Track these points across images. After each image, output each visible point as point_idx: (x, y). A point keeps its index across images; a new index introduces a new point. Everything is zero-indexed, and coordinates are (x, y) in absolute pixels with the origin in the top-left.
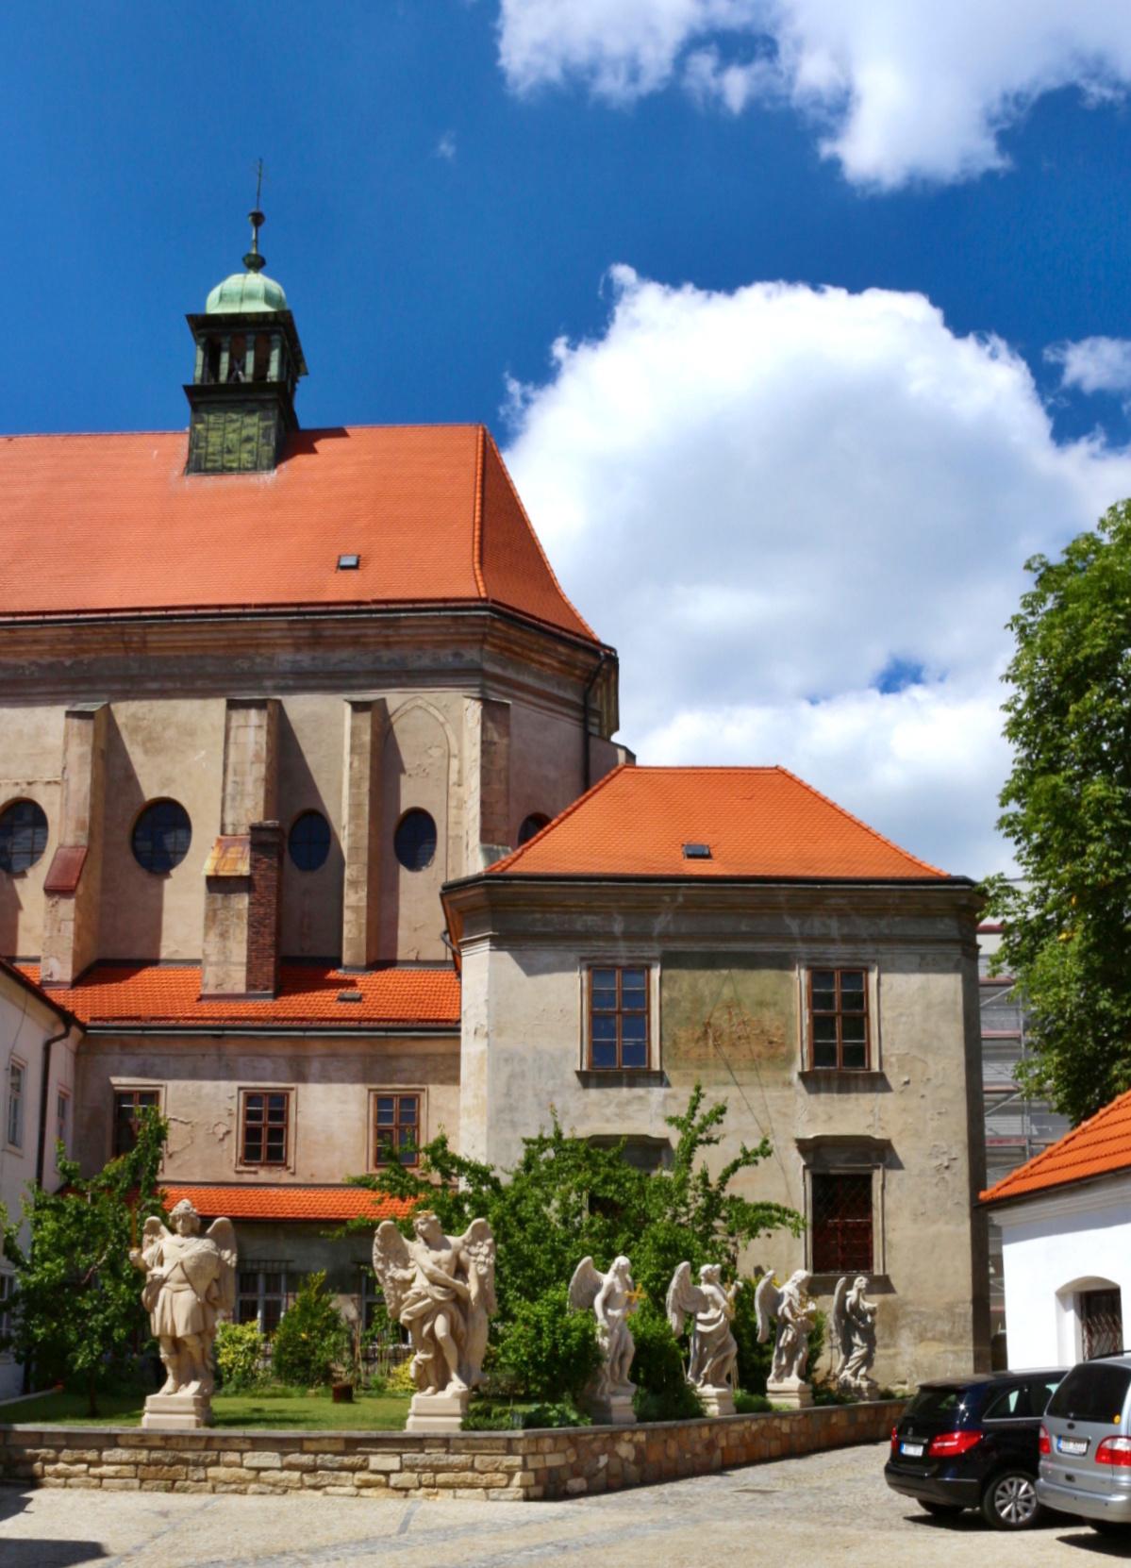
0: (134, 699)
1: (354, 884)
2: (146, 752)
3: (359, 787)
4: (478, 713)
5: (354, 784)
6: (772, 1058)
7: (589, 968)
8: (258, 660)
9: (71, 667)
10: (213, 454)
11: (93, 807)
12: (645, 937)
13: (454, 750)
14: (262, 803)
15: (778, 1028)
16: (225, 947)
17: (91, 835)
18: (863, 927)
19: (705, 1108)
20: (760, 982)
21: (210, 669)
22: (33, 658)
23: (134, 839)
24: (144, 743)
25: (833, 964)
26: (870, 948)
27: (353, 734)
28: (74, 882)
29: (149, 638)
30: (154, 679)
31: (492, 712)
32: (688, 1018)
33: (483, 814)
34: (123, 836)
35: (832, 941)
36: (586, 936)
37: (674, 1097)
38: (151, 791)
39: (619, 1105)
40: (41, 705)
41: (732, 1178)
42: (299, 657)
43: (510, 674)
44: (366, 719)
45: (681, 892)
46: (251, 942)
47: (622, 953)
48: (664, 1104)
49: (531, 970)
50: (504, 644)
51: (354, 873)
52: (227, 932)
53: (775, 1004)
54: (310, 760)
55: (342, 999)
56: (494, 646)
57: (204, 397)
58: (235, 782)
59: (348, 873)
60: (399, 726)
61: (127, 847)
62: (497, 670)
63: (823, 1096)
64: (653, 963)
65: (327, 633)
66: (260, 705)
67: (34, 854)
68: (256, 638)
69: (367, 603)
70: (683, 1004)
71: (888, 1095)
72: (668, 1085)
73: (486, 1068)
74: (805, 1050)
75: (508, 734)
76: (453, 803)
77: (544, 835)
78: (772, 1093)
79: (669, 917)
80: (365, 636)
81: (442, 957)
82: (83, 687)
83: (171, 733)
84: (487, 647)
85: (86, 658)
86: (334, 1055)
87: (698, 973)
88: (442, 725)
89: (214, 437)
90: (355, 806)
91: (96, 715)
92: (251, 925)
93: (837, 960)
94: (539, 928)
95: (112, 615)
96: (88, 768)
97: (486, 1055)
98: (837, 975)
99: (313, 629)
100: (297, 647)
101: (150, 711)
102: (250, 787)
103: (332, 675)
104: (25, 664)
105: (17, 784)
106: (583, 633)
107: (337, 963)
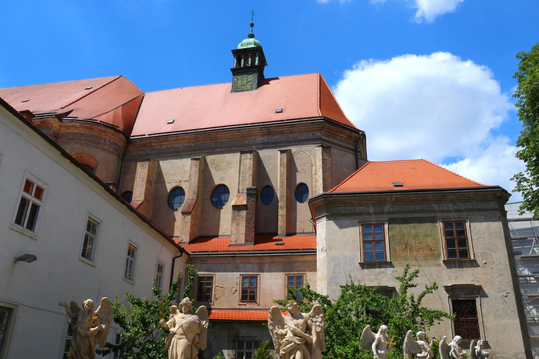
0: (212, 154)
1: (282, 208)
2: (216, 170)
3: (283, 177)
4: (321, 151)
5: (281, 176)
6: (432, 256)
7: (362, 225)
8: (251, 140)
9: (194, 146)
11: (198, 187)
12: (382, 213)
13: (314, 164)
15: (433, 244)
16: (238, 228)
17: (198, 196)
18: (462, 206)
19: (411, 270)
20: (425, 227)
21: (236, 144)
22: (183, 144)
23: (212, 197)
24: (215, 168)
25: (452, 220)
26: (465, 213)
27: (281, 160)
28: (191, 210)
29: (217, 136)
30: (219, 148)
31: (326, 149)
32: (399, 242)
33: (323, 182)
34: (208, 196)
35: (451, 211)
36: (360, 214)
37: (396, 271)
38: (217, 182)
39: (376, 275)
40: (185, 158)
41: (423, 299)
42: (263, 139)
43: (331, 140)
44: (285, 155)
45: (394, 196)
46: (246, 226)
47: (374, 219)
48: (392, 274)
49: (341, 227)
50: (328, 130)
51: (282, 204)
52: (239, 223)
53: (431, 236)
54: (267, 169)
55: (276, 245)
56: (325, 131)
57: (236, 72)
58: (243, 176)
59: (280, 204)
60: (295, 157)
61: (209, 200)
62: (327, 139)
63: (453, 269)
64: (385, 222)
65: (272, 131)
66: (251, 152)
67: (181, 203)
68: (251, 134)
69: (285, 121)
70: (397, 237)
71: (479, 268)
72: (394, 267)
73: (326, 263)
74: (444, 252)
75: (331, 157)
76: (314, 180)
77: (344, 183)
78: (433, 269)
79: (390, 205)
80: (284, 130)
81: (312, 231)
82: (197, 152)
83: (224, 164)
84: (323, 132)
85: (198, 143)
86: (273, 262)
87: (402, 225)
89: (239, 82)
90: (282, 183)
91: (200, 159)
92: (246, 221)
93: (453, 218)
94: (343, 212)
96: (197, 175)
97: (326, 258)
98: (454, 224)
99: (268, 130)
100: (263, 135)
101: (218, 158)
103: (273, 143)
104: (181, 146)
105: (176, 182)
107: (276, 234)
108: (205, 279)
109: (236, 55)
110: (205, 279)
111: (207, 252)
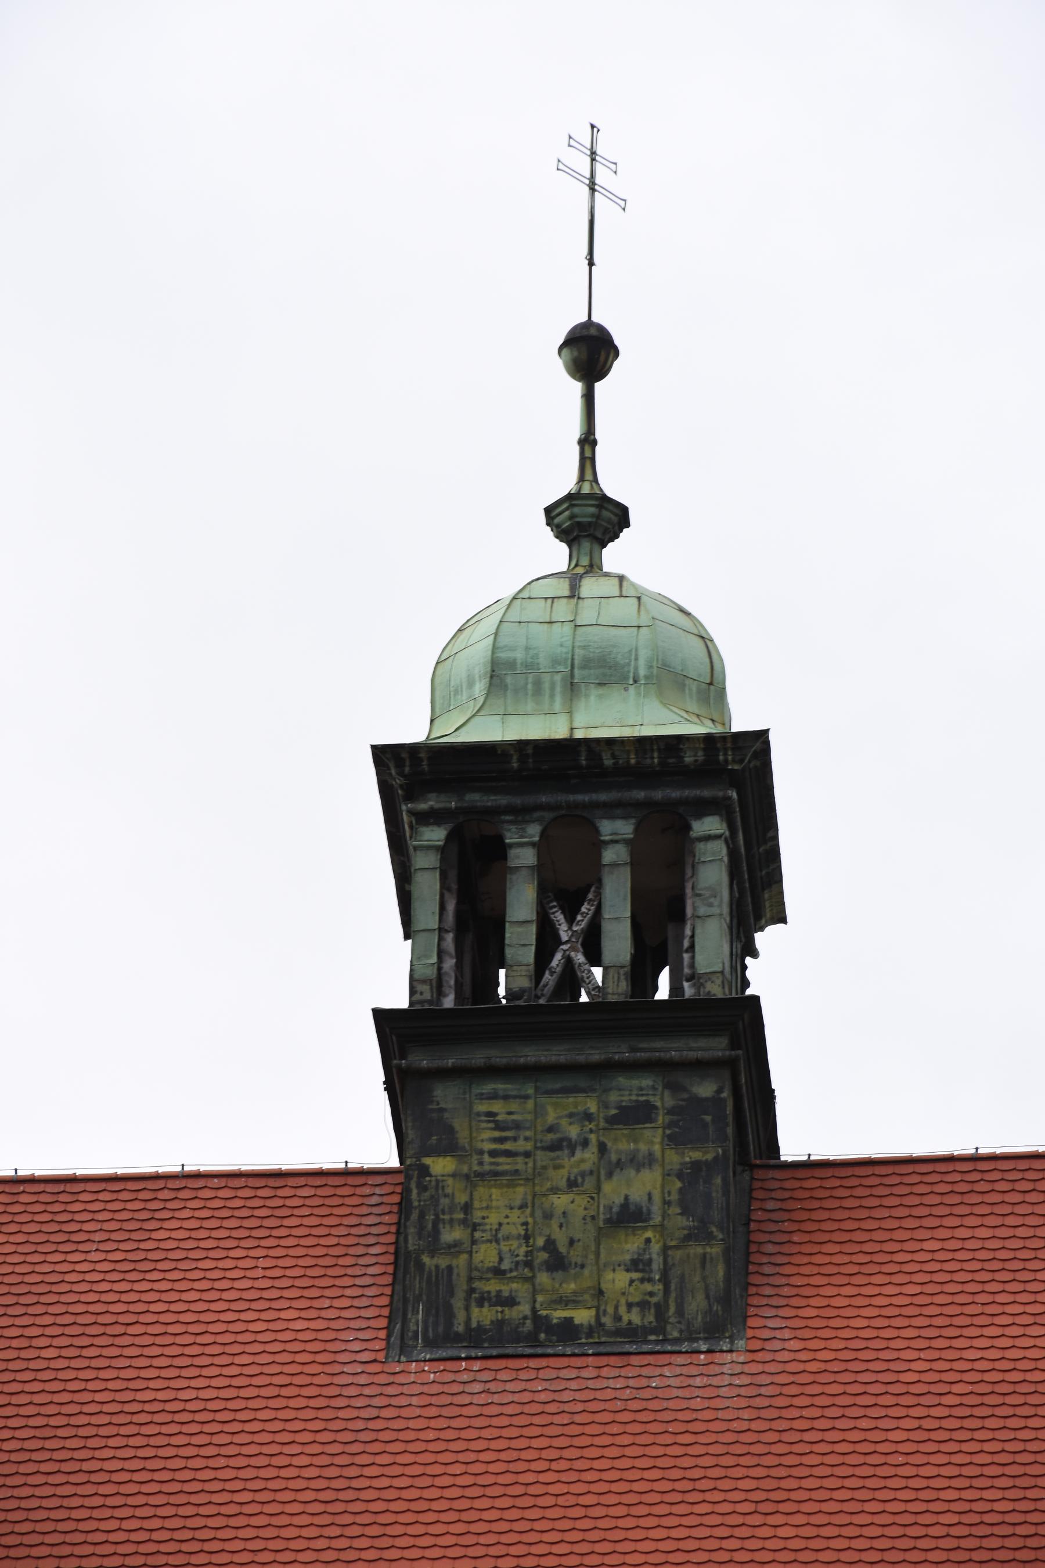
10: (498, 1272)
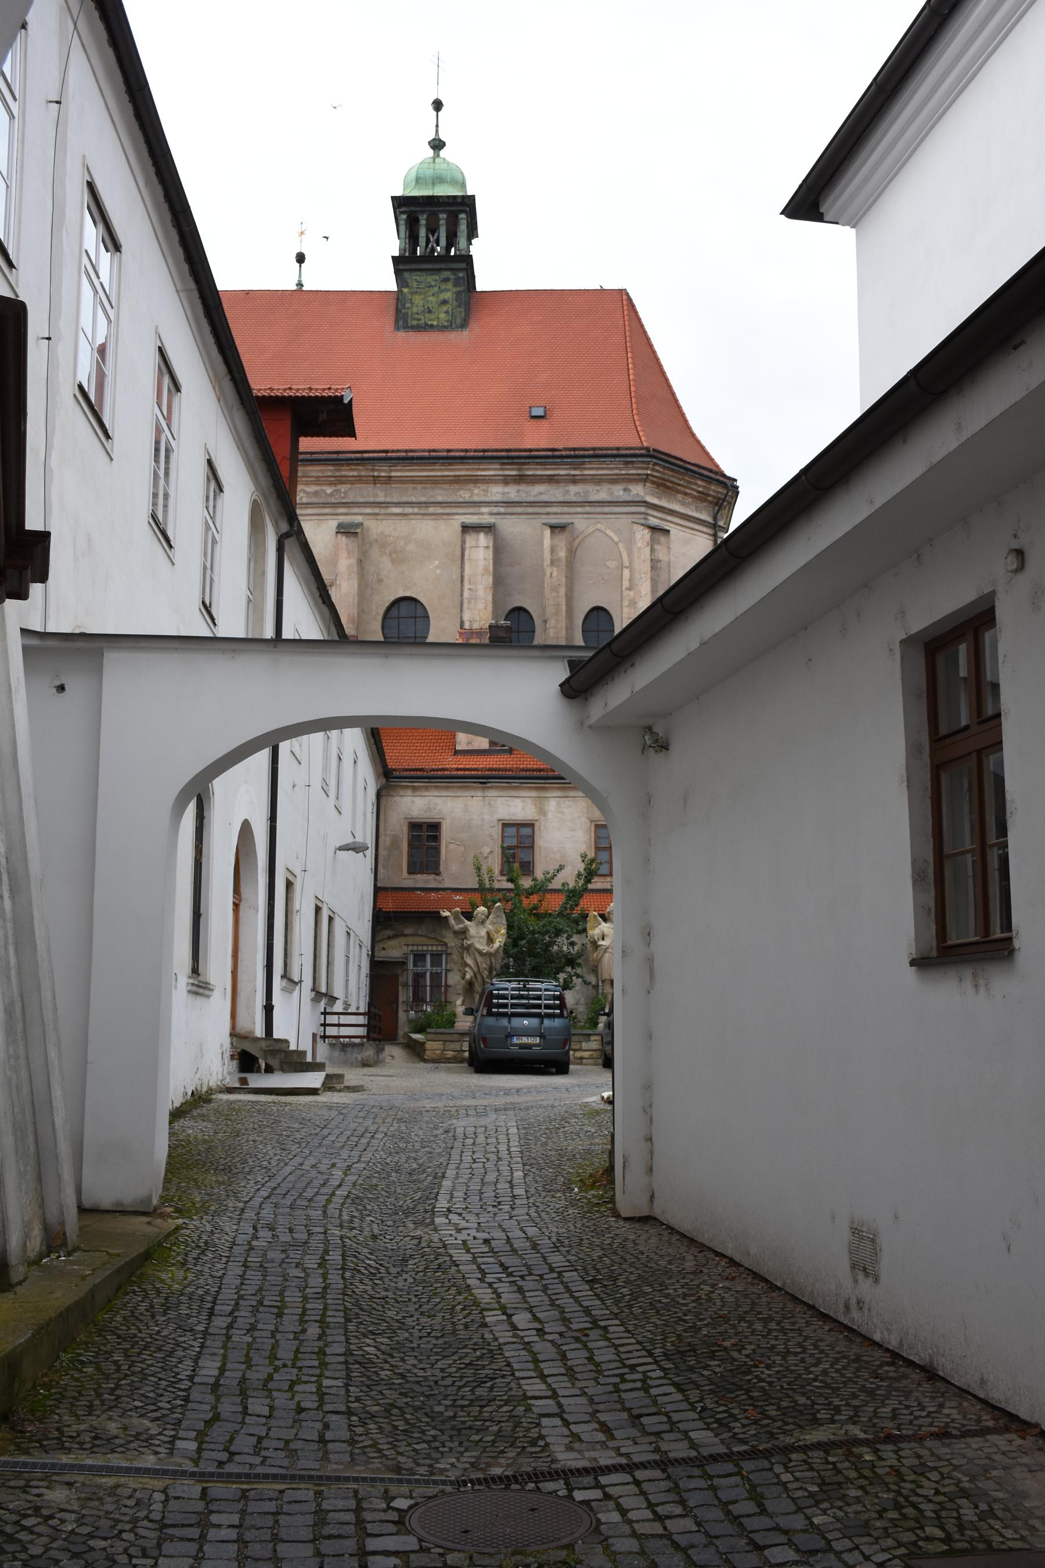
2: (393, 561)
3: (557, 592)
9: (332, 495)
14: (490, 605)
24: (391, 555)
27: (553, 550)
83: (411, 547)
88: (616, 544)
89: (418, 300)
95: (367, 455)
101: (395, 530)
102: (481, 593)
106: (714, 468)
108: (425, 826)
109: (402, 213)
110: (425, 826)
111: (421, 770)
